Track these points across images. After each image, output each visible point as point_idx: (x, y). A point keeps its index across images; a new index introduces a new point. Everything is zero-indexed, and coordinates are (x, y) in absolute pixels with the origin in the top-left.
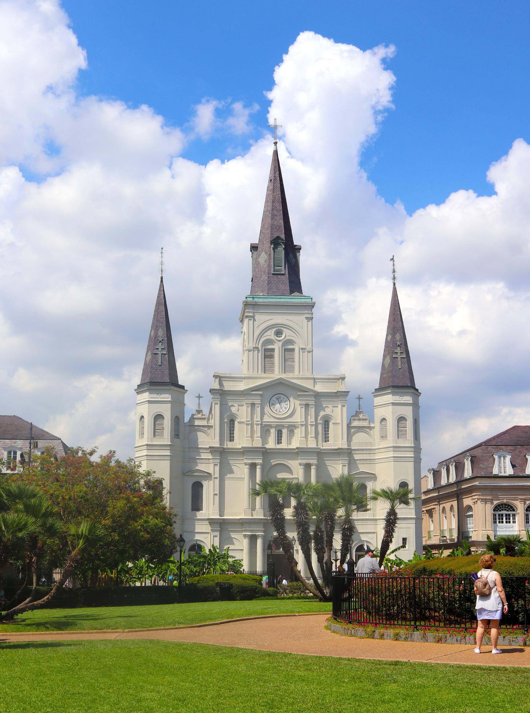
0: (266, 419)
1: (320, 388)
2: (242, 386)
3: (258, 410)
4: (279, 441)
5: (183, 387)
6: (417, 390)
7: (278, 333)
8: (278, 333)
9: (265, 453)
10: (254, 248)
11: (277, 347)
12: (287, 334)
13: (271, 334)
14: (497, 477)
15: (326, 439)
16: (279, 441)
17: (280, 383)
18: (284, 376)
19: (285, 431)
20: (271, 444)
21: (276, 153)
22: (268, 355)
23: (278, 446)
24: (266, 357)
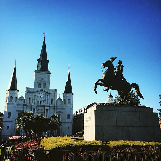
3: (36, 96)
4: (41, 104)
5: (18, 90)
7: (42, 79)
8: (42, 79)
11: (42, 82)
12: (45, 80)
13: (40, 79)
16: (41, 104)
18: (43, 89)
20: (39, 104)
21: (45, 39)
22: (40, 84)
24: (39, 84)
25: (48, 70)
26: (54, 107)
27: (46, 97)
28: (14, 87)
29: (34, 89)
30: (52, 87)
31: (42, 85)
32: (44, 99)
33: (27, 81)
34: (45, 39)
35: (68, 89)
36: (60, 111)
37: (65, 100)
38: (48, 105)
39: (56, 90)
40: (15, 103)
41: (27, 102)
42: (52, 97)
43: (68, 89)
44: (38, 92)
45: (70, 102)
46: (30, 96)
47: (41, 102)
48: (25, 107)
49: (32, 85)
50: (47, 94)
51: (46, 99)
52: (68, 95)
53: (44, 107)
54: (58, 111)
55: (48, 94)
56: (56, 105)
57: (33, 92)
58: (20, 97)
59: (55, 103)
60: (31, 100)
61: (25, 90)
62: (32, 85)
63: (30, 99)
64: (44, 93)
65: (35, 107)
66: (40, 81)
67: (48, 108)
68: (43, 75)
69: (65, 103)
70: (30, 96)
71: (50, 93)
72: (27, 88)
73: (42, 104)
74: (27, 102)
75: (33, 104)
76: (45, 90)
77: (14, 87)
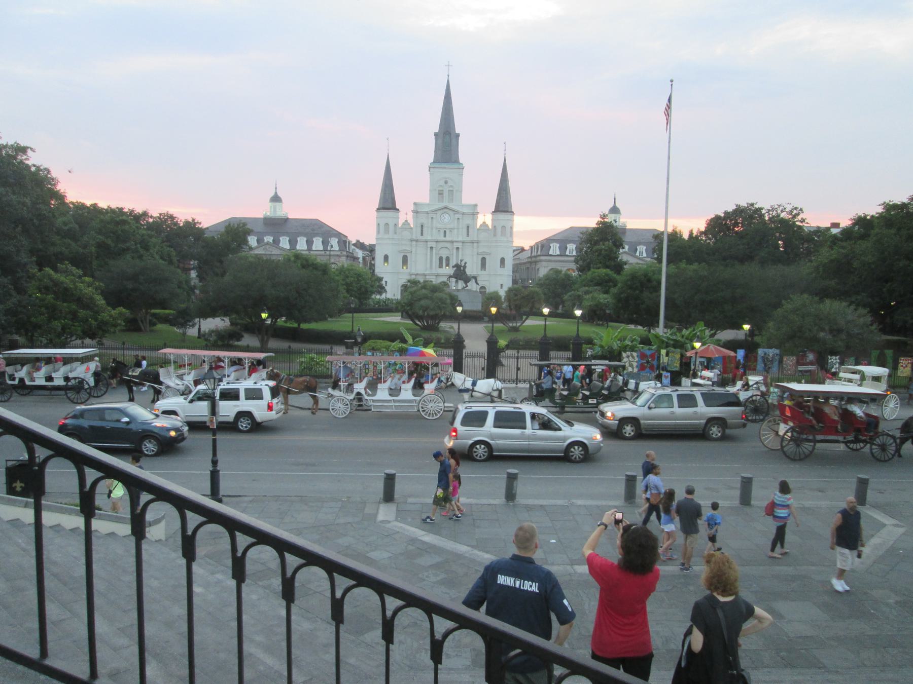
0: (439, 226)
1: (465, 211)
2: (426, 209)
4: (445, 236)
7: (446, 182)
8: (446, 182)
9: (437, 242)
10: (436, 135)
11: (446, 189)
12: (450, 183)
13: (442, 183)
14: (551, 255)
15: (468, 235)
16: (445, 236)
17: (446, 208)
20: (442, 238)
21: (448, 82)
22: (441, 193)
25: (457, 161)
26: (473, 242)
27: (456, 221)
28: (388, 203)
29: (428, 205)
30: (467, 198)
31: (446, 194)
32: (452, 226)
33: (413, 190)
34: (448, 82)
35: (503, 206)
36: (485, 250)
37: (495, 227)
38: (460, 239)
39: (476, 205)
41: (416, 234)
42: (468, 221)
43: (503, 206)
44: (439, 213)
45: (507, 231)
46: (423, 219)
48: (414, 243)
49: (424, 196)
50: (457, 216)
52: (502, 216)
53: (452, 242)
54: (481, 250)
55: (460, 216)
56: (476, 239)
57: (427, 213)
58: (403, 224)
59: (473, 236)
60: (424, 229)
61: (412, 207)
62: (424, 196)
63: (422, 226)
64: (451, 212)
65: (433, 245)
66: (441, 186)
67: (460, 245)
68: (446, 172)
69: (495, 235)
70: (423, 219)
71: (463, 214)
72: (415, 204)
73: (448, 238)
74: (416, 234)
75: (429, 238)
76: (451, 206)
77: (388, 203)
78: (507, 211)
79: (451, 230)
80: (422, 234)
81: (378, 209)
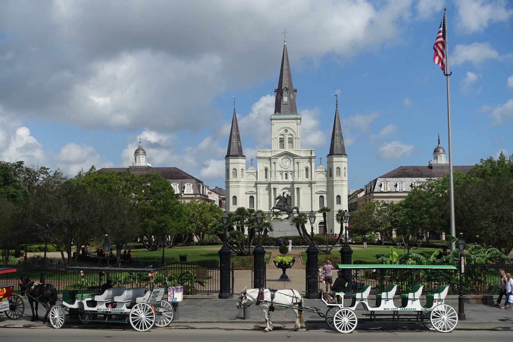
4: (286, 178)
5: (244, 156)
6: (346, 155)
7: (286, 131)
8: (286, 131)
12: (290, 132)
13: (283, 131)
16: (286, 178)
19: (289, 174)
23: (286, 180)
24: (280, 141)
38: (300, 180)
40: (242, 180)
44: (280, 159)
47: (286, 174)
51: (296, 168)
57: (270, 159)
71: (302, 158)
73: (290, 179)
78: (341, 154)
79: (293, 172)
80: (266, 177)
81: (226, 156)
